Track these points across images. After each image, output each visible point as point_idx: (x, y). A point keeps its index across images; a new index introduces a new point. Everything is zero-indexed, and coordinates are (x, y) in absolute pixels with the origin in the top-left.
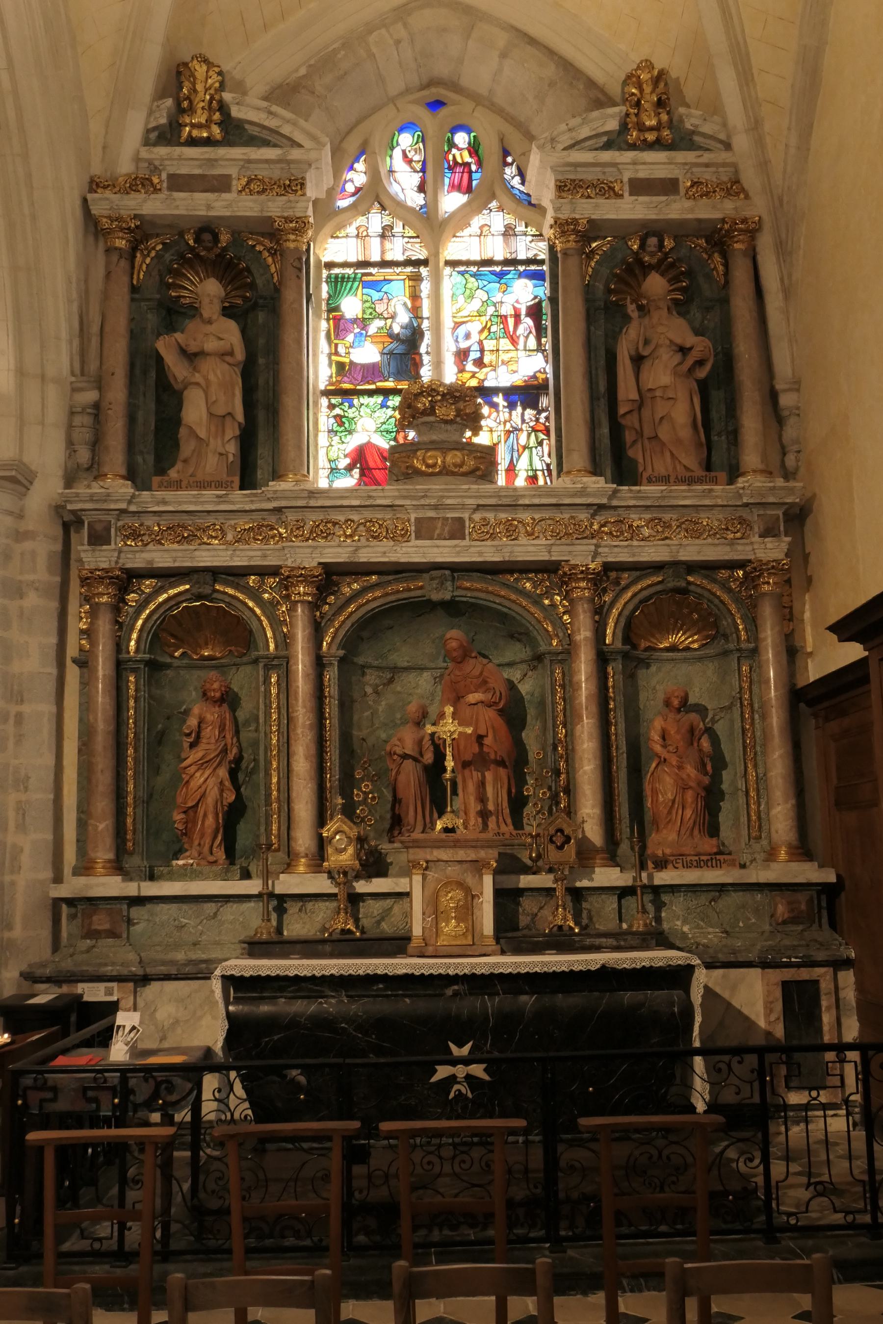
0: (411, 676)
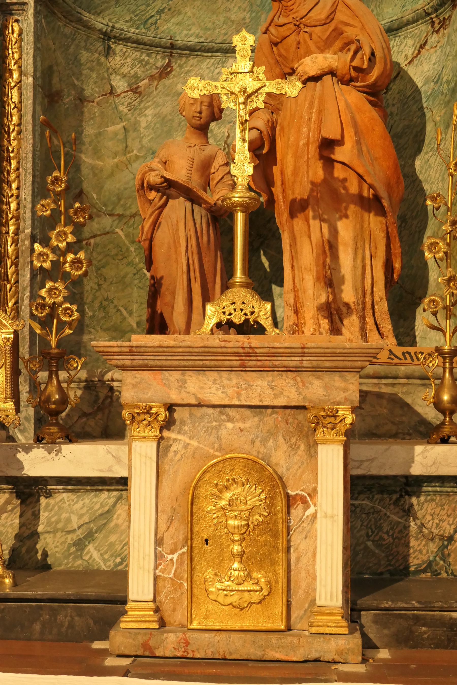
0: (204, 65)
